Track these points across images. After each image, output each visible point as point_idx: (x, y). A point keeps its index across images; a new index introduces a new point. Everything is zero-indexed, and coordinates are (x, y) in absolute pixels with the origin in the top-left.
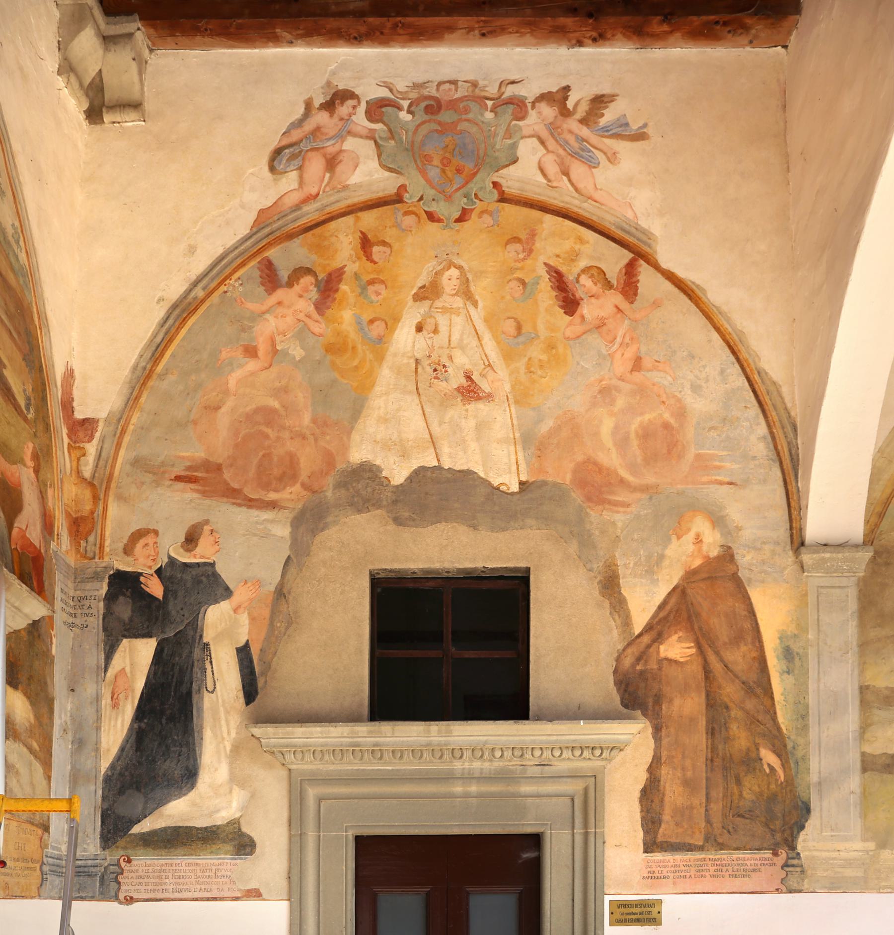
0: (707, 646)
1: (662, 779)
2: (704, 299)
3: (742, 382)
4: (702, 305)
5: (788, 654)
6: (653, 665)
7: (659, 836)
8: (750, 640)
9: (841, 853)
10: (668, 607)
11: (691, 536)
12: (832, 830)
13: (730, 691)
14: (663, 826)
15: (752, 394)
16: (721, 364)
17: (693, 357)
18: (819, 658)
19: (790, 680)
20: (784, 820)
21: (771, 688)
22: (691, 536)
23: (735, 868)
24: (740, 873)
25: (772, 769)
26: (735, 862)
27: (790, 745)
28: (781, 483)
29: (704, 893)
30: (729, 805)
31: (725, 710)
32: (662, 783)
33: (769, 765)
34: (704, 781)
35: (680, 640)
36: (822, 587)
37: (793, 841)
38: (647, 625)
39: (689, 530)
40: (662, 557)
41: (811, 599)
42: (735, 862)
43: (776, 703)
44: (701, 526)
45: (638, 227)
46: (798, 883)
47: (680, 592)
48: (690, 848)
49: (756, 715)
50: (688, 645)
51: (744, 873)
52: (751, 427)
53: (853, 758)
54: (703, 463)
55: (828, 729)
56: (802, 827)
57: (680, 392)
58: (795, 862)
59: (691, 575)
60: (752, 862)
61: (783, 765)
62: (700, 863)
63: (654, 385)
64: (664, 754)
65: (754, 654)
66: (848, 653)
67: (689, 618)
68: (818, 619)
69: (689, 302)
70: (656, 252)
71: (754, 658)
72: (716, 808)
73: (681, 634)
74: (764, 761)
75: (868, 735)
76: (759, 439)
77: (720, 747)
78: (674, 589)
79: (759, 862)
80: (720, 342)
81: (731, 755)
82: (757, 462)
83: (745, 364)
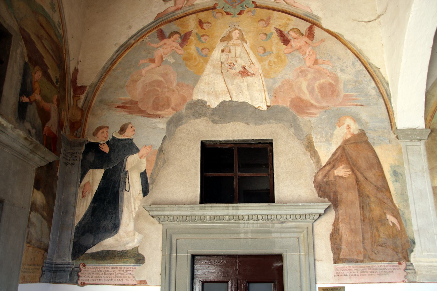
0: (356, 171)
1: (340, 229)
2: (343, 38)
3: (362, 67)
4: (342, 41)
5: (395, 173)
6: (332, 179)
7: (341, 255)
8: (376, 168)
9: (433, 263)
10: (337, 155)
11: (345, 125)
12: (428, 252)
13: (369, 189)
14: (342, 251)
15: (367, 72)
16: (352, 61)
17: (340, 59)
18: (410, 175)
19: (398, 184)
20: (402, 247)
21: (389, 188)
22: (345, 125)
23: (380, 271)
24: (383, 273)
25: (393, 224)
26: (380, 268)
27: (401, 213)
28: (384, 105)
29: (365, 283)
30: (374, 240)
31: (368, 198)
32: (340, 231)
33: (392, 222)
34: (361, 230)
35: (343, 168)
36: (408, 145)
37: (408, 257)
38: (328, 162)
39: (344, 124)
40: (332, 134)
41: (403, 150)
42: (380, 268)
43: (392, 195)
44: (349, 121)
45: (313, 15)
46: (413, 278)
47: (342, 148)
48: (357, 261)
49: (383, 200)
50: (347, 170)
51: (385, 273)
52: (368, 84)
54: (347, 98)
56: (412, 251)
57: (336, 72)
58: (410, 267)
59: (346, 142)
60: (389, 268)
61: (398, 222)
62: (362, 268)
63: (324, 69)
64: (340, 218)
65: (379, 174)
66: (424, 173)
67: (347, 159)
68: (408, 159)
69: (336, 40)
70: (321, 23)
71: (379, 176)
72: (368, 242)
73: (344, 165)
74: (389, 220)
77: (367, 214)
78: (339, 147)
79: (392, 268)
80: (351, 54)
81: (373, 218)
82: (372, 97)
83: (363, 61)
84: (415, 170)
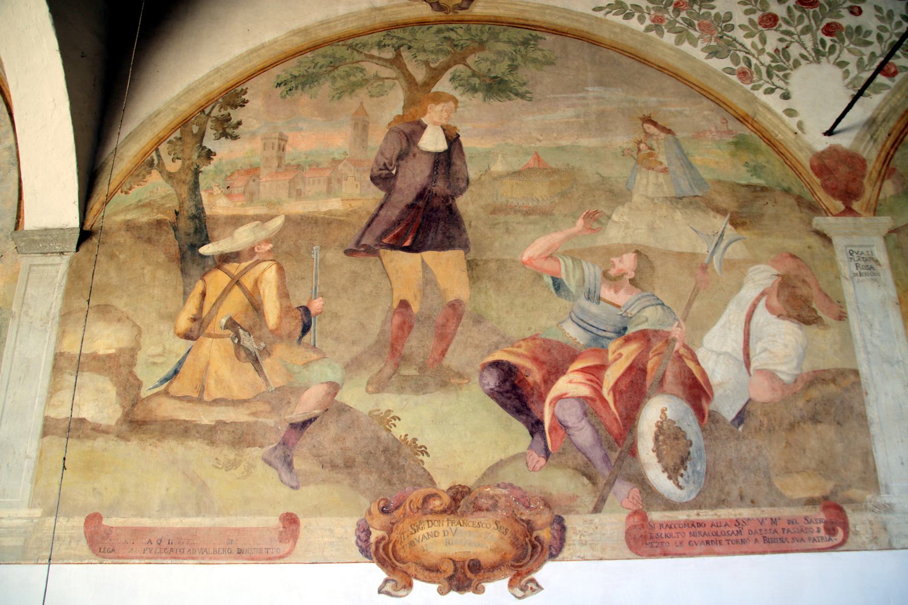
18: (18, 328)
36: (34, 265)
41: (22, 276)
53: (36, 424)
55: (15, 394)
66: (48, 323)
75: (55, 400)
76: (5, 148)
84: (31, 317)
